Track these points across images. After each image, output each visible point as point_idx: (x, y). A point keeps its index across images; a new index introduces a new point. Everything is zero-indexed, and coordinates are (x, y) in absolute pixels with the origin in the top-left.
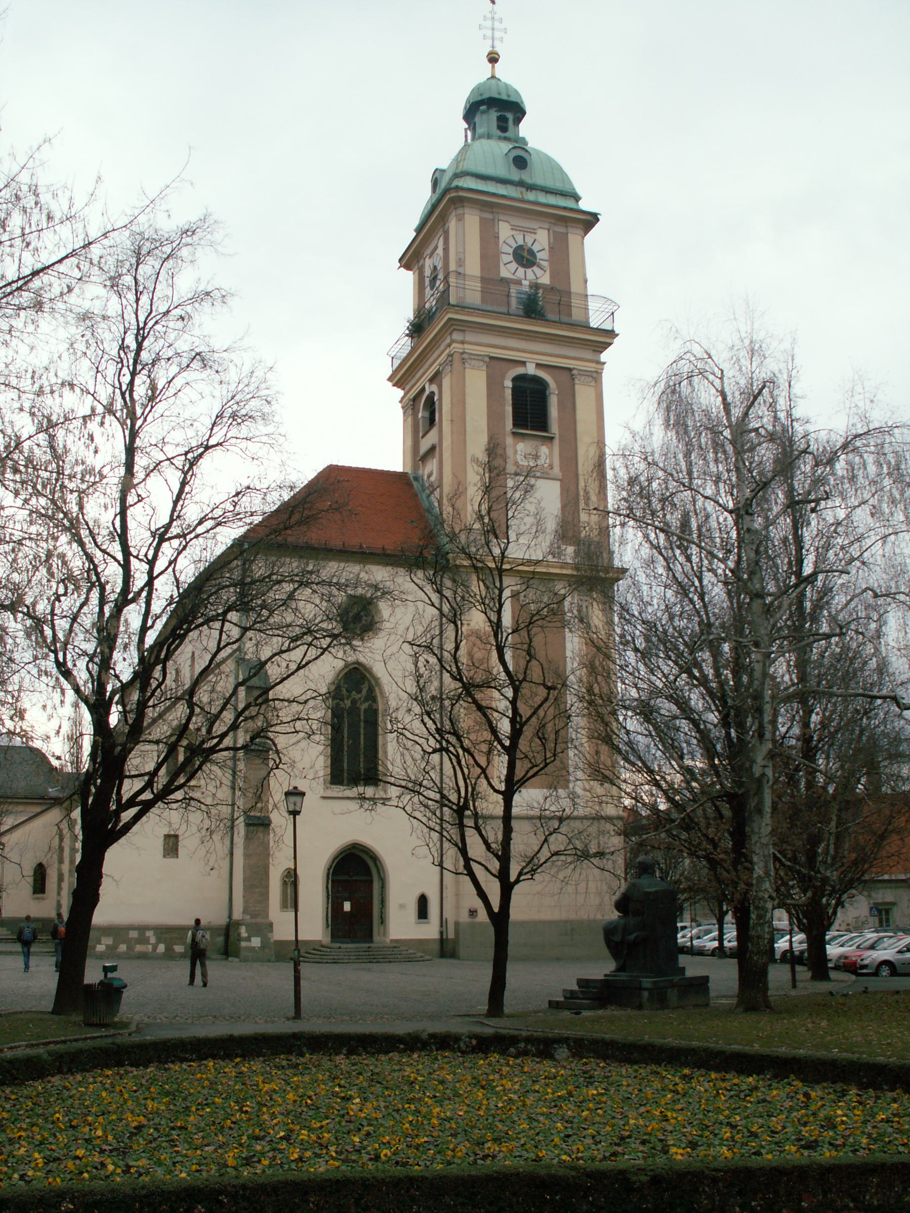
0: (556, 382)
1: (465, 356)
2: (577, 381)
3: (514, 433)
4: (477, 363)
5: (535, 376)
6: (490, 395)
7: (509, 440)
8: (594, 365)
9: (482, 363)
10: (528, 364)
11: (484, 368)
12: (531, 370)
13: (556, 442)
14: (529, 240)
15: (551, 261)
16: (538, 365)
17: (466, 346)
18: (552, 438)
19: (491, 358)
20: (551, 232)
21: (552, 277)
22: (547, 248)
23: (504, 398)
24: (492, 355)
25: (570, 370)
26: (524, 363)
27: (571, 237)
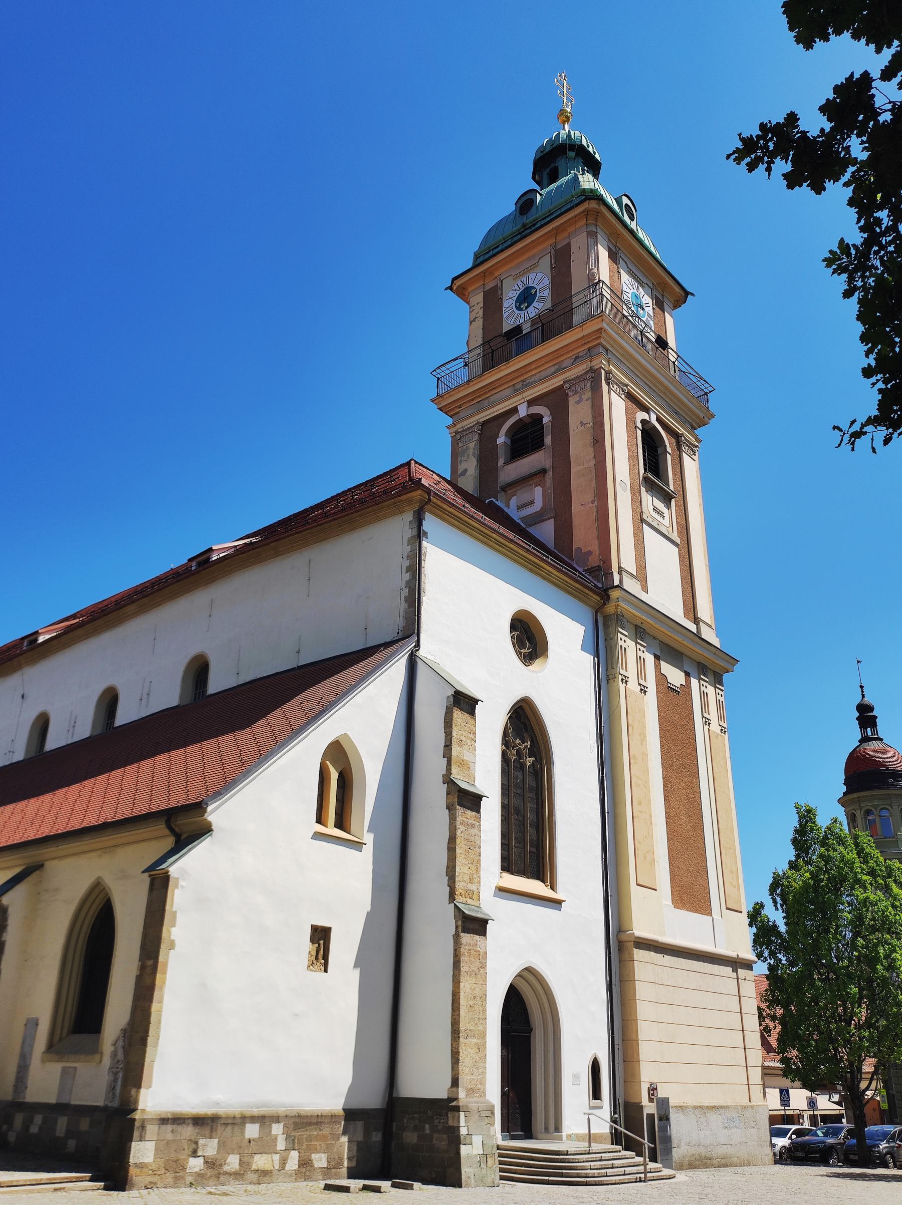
12: (523, 411)
16: (531, 403)
17: (459, 426)
19: (484, 423)
24: (481, 421)
25: (561, 387)
26: (515, 410)
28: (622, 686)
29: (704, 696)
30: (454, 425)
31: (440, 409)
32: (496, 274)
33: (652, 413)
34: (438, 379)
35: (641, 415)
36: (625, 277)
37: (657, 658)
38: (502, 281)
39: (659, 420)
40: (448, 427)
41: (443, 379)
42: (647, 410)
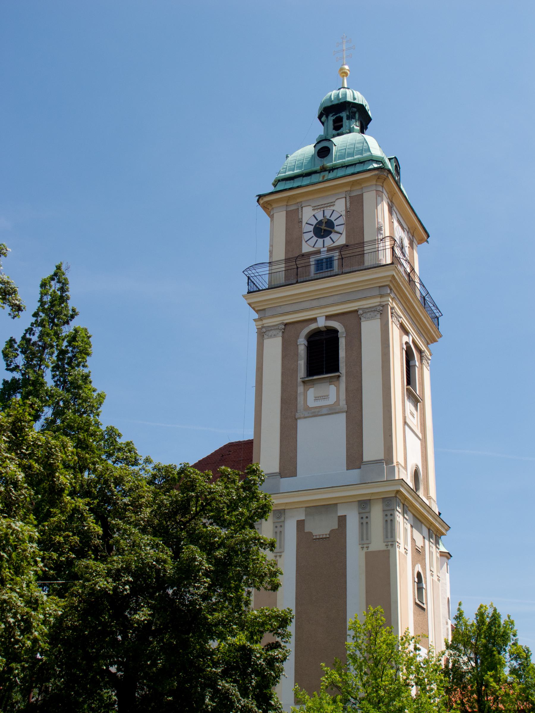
0: (345, 326)
1: (264, 330)
2: (363, 319)
3: (304, 382)
4: (274, 332)
5: (325, 327)
6: (284, 356)
7: (301, 389)
8: (378, 300)
9: (278, 331)
10: (318, 319)
11: (281, 334)
12: (322, 323)
13: (343, 379)
14: (328, 214)
15: (347, 224)
16: (328, 317)
17: (265, 321)
18: (339, 376)
19: (286, 325)
20: (348, 198)
21: (347, 237)
22: (343, 213)
23: (297, 354)
24: (286, 322)
25: (356, 311)
26: (314, 320)
27: (365, 196)
28: (397, 549)
29: (431, 553)
30: (260, 319)
31: (249, 304)
32: (298, 201)
33: (410, 335)
34: (249, 278)
35: (405, 338)
36: (396, 224)
37: (412, 526)
38: (302, 208)
39: (414, 342)
40: (255, 320)
41: (251, 278)
42: (407, 333)
